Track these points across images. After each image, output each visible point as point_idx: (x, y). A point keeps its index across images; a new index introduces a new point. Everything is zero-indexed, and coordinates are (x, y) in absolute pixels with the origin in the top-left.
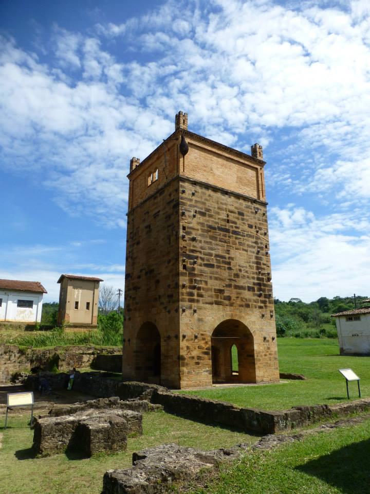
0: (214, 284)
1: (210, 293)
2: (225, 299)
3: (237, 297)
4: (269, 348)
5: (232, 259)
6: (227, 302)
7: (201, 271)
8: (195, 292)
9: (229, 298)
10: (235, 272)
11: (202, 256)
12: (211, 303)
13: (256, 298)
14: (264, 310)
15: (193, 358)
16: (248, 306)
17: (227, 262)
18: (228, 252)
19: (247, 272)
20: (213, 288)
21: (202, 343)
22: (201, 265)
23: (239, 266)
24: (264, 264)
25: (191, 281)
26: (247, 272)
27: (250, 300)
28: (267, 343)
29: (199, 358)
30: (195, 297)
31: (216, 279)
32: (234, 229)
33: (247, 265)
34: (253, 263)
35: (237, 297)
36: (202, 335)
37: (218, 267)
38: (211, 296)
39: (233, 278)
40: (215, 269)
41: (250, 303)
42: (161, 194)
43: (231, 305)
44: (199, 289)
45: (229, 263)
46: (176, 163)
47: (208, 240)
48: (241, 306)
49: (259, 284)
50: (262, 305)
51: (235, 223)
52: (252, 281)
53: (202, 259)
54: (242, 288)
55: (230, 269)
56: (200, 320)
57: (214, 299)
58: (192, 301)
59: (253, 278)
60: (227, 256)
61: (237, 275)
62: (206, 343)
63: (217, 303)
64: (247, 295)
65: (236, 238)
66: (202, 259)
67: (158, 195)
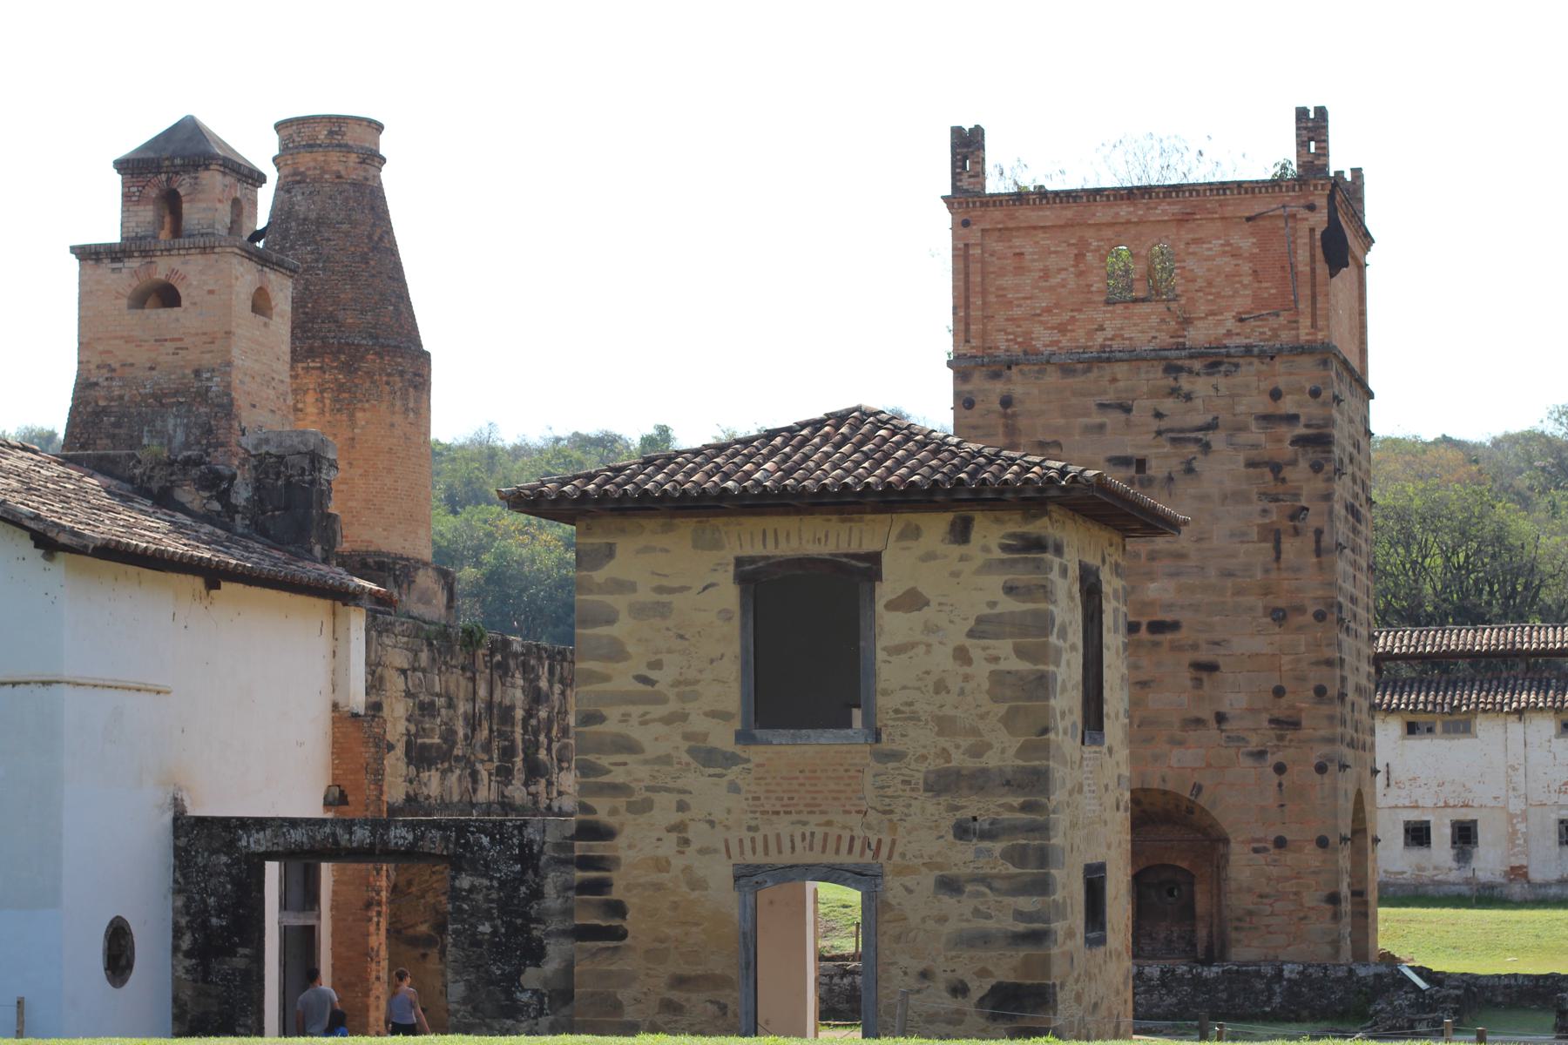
42: (1213, 367)
46: (1307, 291)
67: (1197, 365)
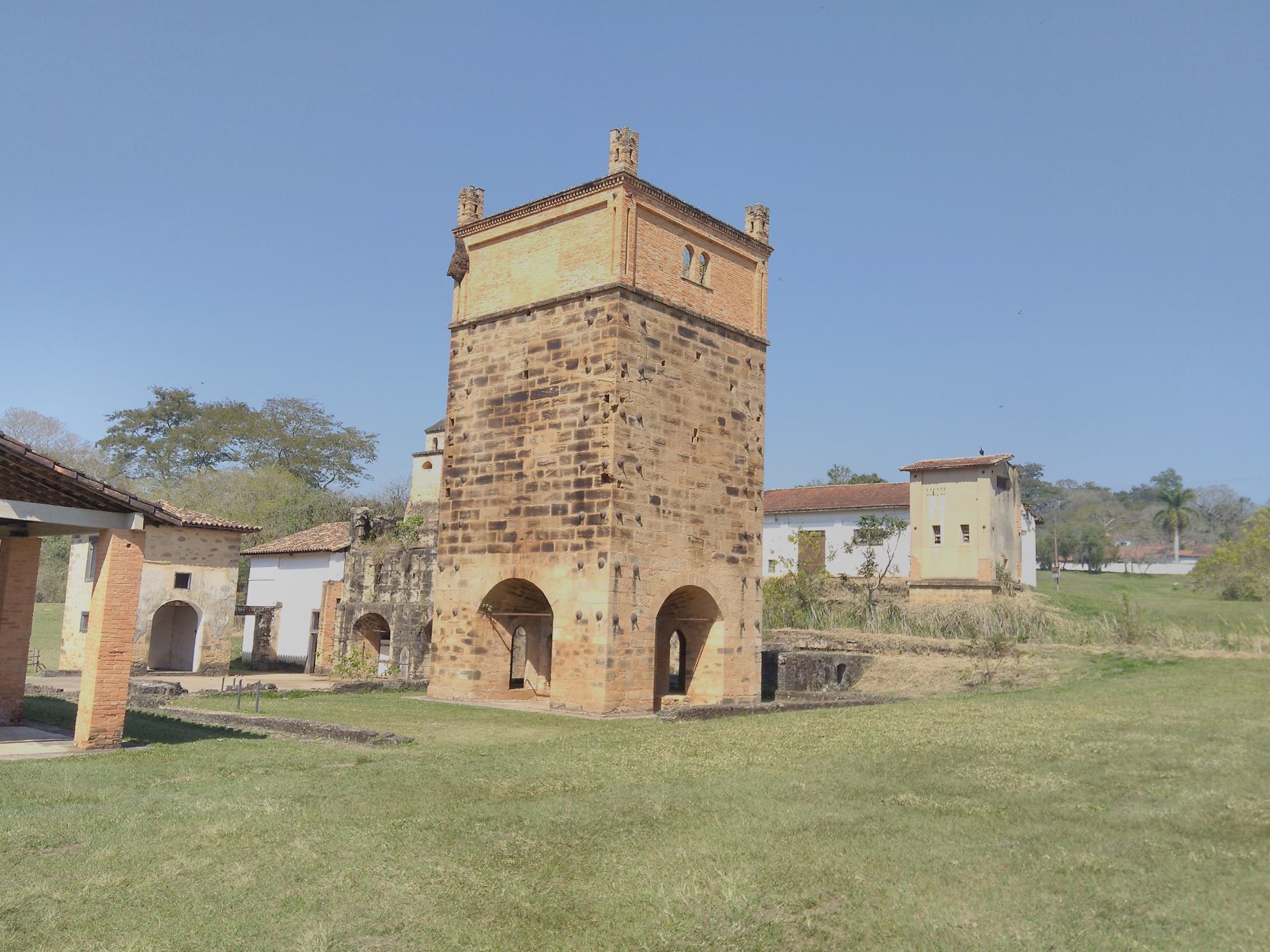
0: (490, 513)
1: (481, 532)
2: (505, 540)
3: (529, 533)
4: (585, 639)
5: (524, 454)
6: (509, 545)
7: (471, 493)
8: (460, 533)
9: (512, 537)
10: (530, 480)
11: (475, 464)
12: (482, 551)
13: (567, 528)
14: (584, 551)
15: (448, 648)
16: (549, 548)
17: (511, 462)
18: (520, 441)
19: (553, 473)
20: (488, 520)
21: (462, 624)
22: (471, 483)
23: (539, 465)
24: (597, 445)
25: (455, 516)
26: (553, 473)
27: (554, 535)
28: (584, 627)
29: (457, 649)
30: (459, 544)
31: (495, 502)
32: (537, 387)
33: (557, 458)
34: (571, 448)
35: (529, 533)
36: (464, 609)
37: (500, 478)
38: (483, 538)
39: (524, 494)
40: (494, 485)
41: (554, 542)
43: (516, 549)
44: (465, 527)
45: (520, 465)
47: (487, 430)
48: (536, 549)
49: (579, 496)
50: (582, 541)
51: (541, 371)
52: (563, 491)
53: (476, 470)
54: (542, 511)
55: (520, 476)
56: (463, 583)
57: (486, 544)
58: (453, 550)
59: (567, 484)
60: (518, 450)
61: (533, 487)
62: (469, 623)
63: (492, 550)
64: (551, 524)
65: (539, 406)
66: (476, 470)
